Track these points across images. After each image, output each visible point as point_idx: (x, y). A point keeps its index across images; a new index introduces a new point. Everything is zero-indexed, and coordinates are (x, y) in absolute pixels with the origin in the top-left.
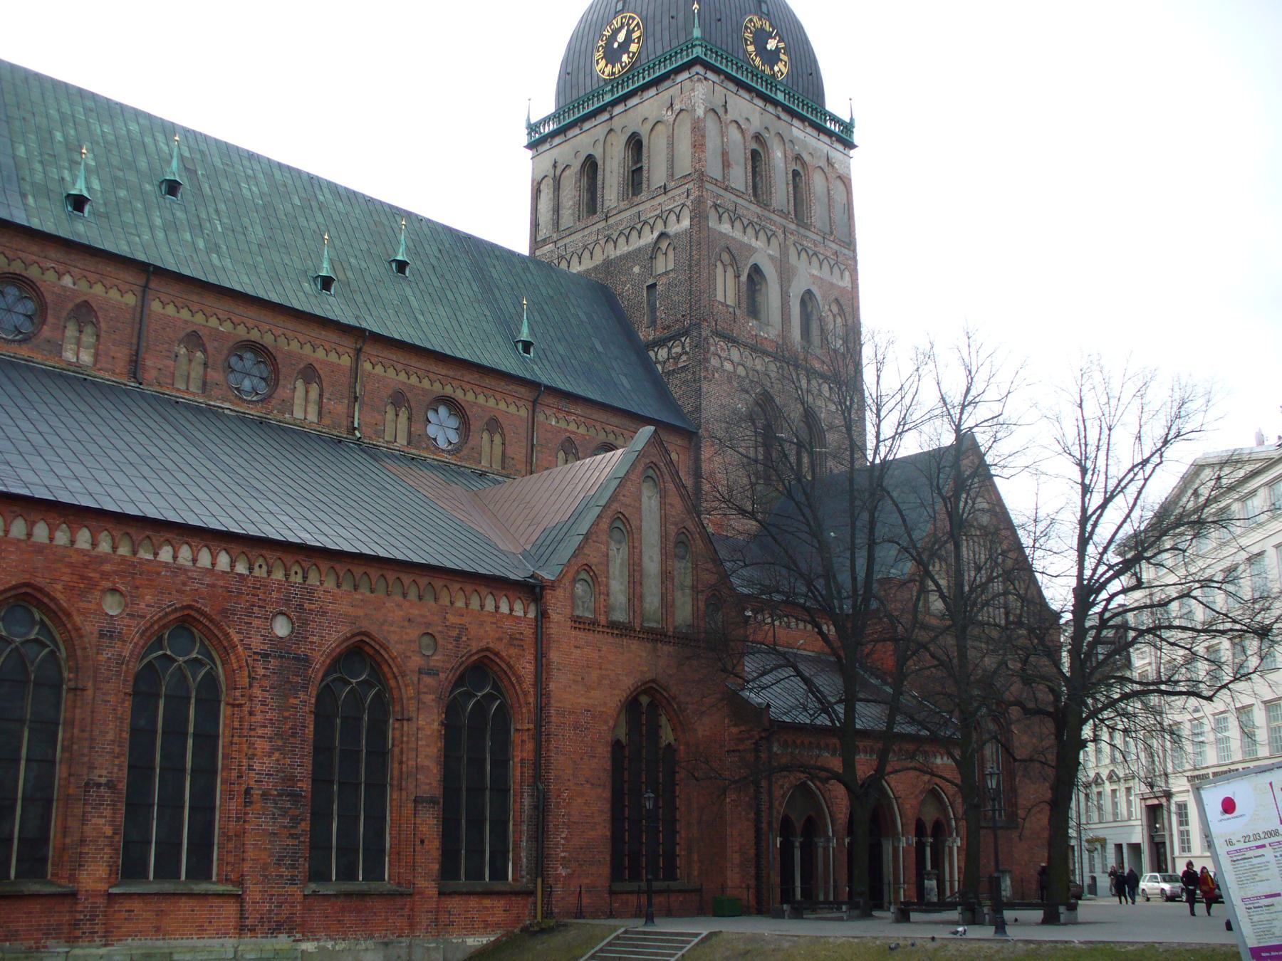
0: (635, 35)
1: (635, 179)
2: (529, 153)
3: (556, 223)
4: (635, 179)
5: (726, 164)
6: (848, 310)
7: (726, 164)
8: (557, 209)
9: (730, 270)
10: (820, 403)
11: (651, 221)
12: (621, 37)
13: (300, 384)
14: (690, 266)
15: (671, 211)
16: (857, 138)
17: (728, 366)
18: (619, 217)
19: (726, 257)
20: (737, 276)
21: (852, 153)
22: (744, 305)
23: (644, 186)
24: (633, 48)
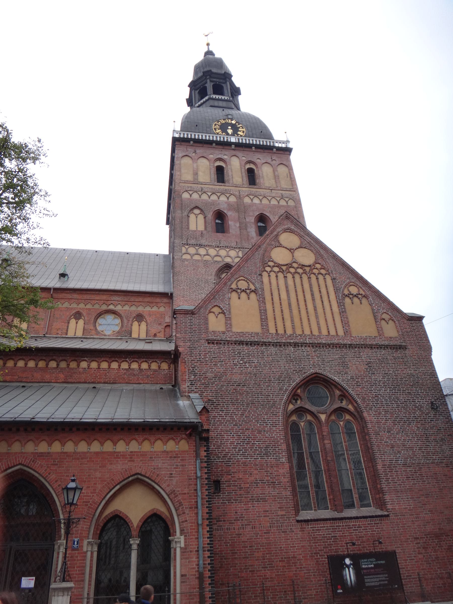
2: (168, 226)
7: (196, 174)
9: (201, 217)
16: (290, 146)
17: (196, 257)
19: (197, 211)
20: (205, 218)
22: (209, 229)
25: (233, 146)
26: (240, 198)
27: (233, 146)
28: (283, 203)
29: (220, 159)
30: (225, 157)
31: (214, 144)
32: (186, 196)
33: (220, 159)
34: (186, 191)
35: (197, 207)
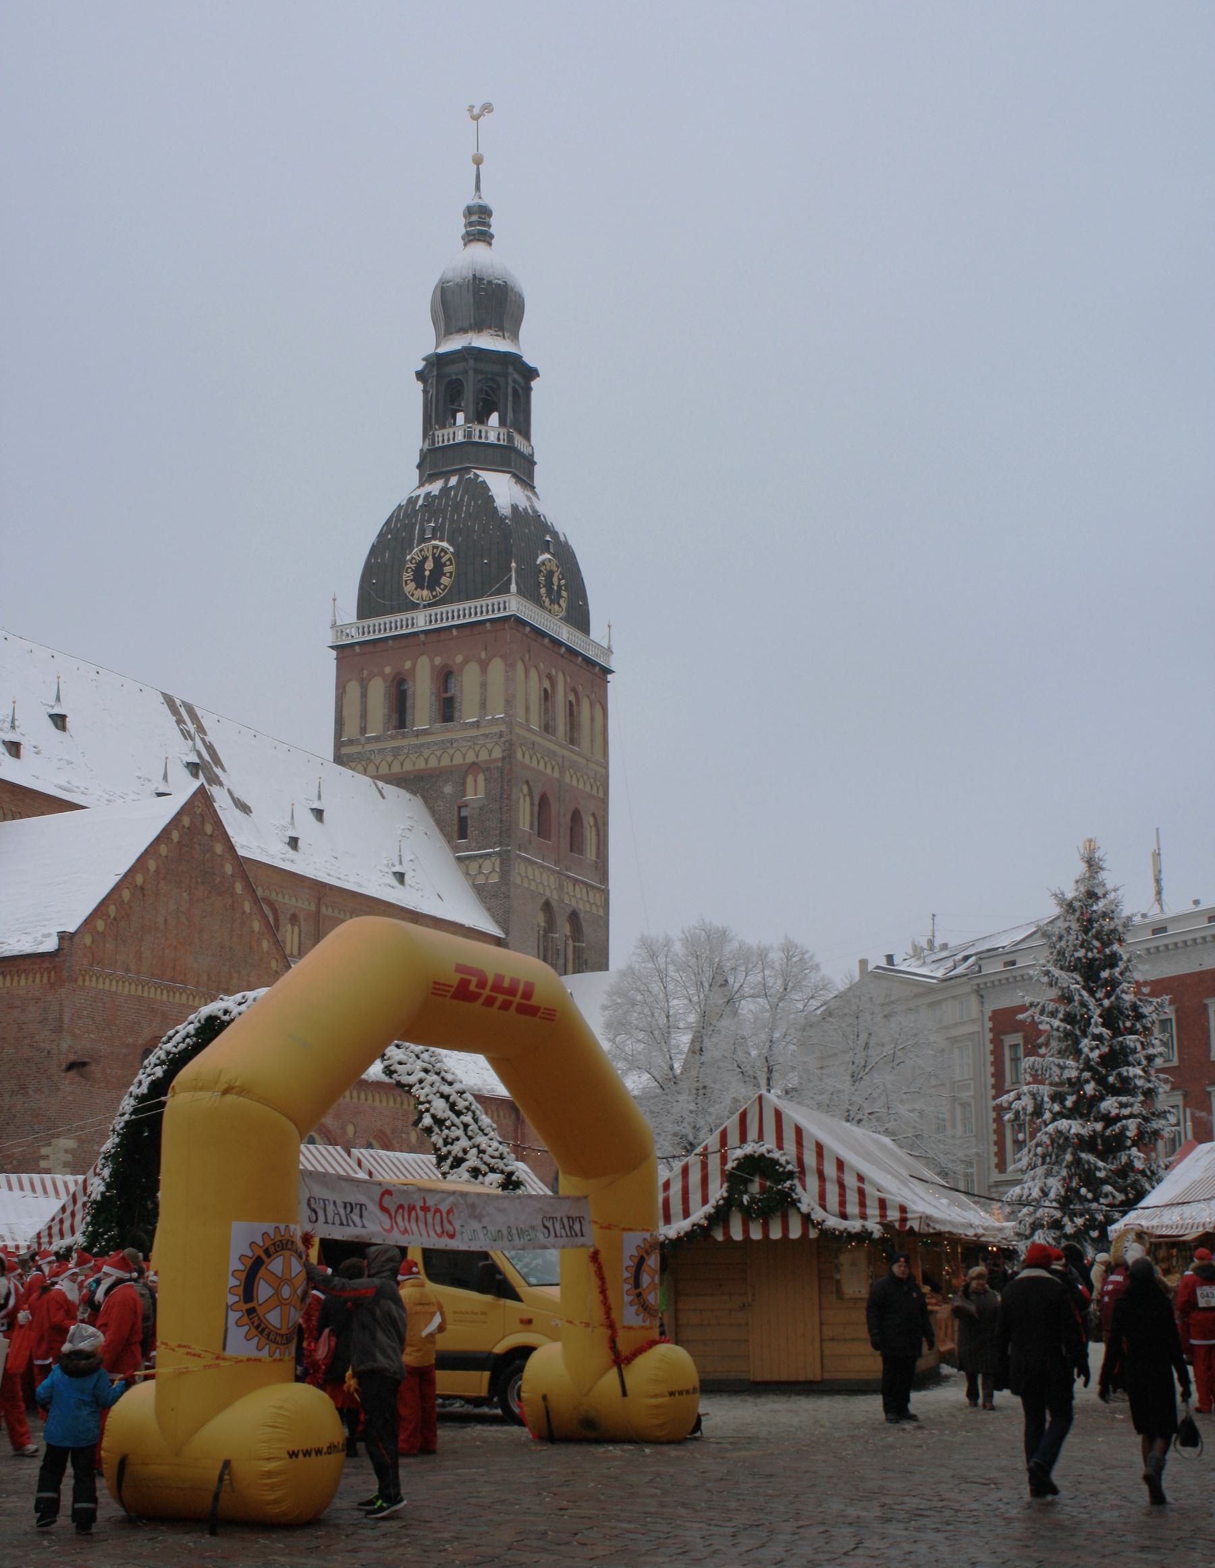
0: (447, 569)
1: (447, 710)
2: (334, 653)
3: (363, 730)
4: (447, 710)
5: (527, 709)
6: (600, 822)
7: (527, 709)
8: (364, 715)
9: (527, 799)
10: (581, 905)
11: (464, 750)
12: (429, 565)
13: (289, 927)
14: (501, 798)
15: (484, 745)
18: (430, 739)
19: (525, 789)
20: (532, 804)
21: (609, 677)
23: (457, 714)
24: (445, 580)
25: (563, 650)
26: (562, 772)
27: (563, 650)
28: (594, 792)
29: (549, 676)
30: (554, 673)
31: (547, 640)
32: (519, 755)
33: (549, 676)
34: (521, 745)
35: (527, 783)
